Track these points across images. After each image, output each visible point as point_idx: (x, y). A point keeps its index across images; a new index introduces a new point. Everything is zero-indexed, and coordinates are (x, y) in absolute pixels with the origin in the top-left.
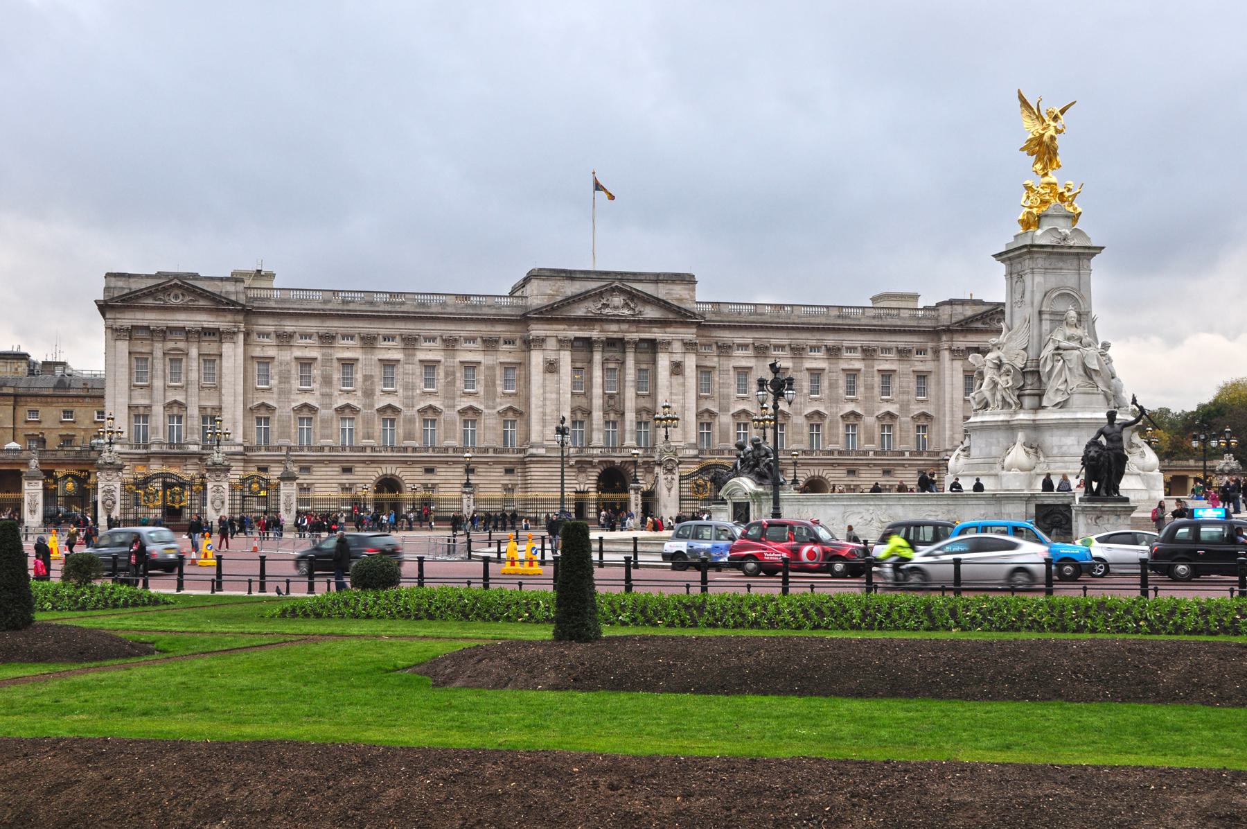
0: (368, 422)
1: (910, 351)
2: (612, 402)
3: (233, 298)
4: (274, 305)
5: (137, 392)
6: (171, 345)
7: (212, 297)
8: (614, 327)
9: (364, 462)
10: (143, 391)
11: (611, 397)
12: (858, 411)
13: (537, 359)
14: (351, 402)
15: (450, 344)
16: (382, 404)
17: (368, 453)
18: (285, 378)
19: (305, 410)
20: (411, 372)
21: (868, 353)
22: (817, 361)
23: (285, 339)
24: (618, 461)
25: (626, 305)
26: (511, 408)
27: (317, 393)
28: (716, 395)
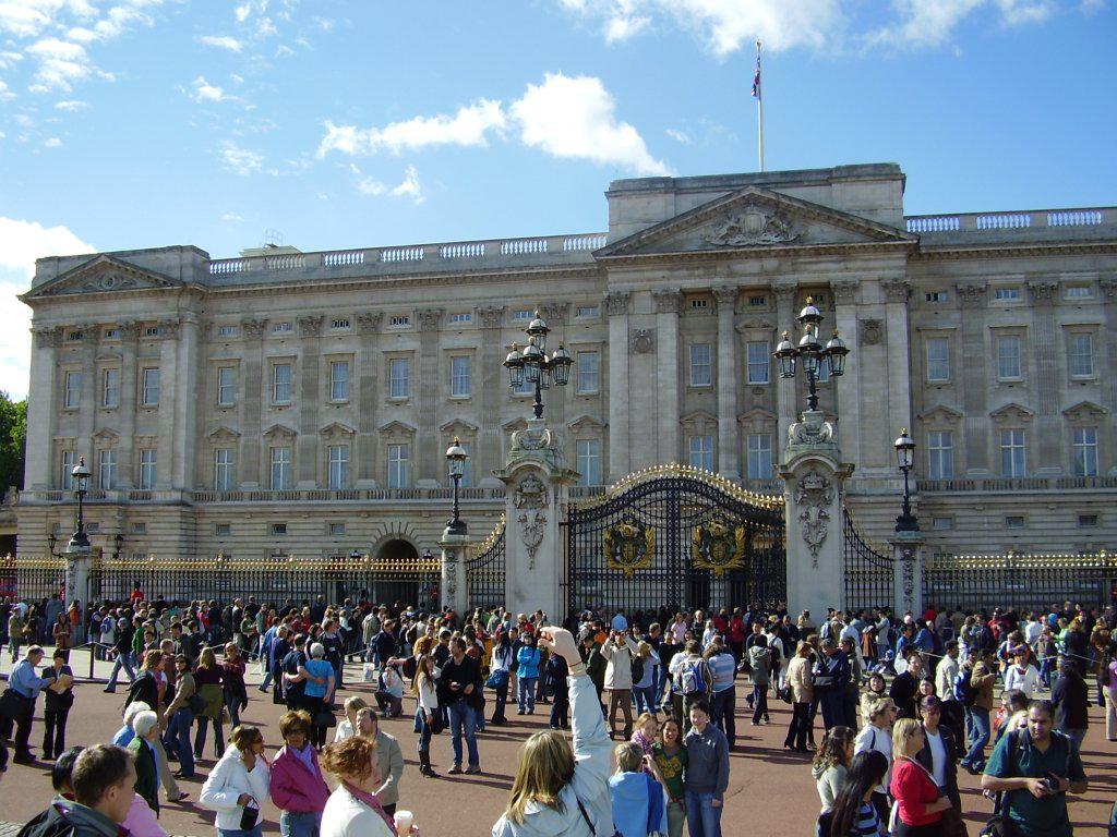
0: (368, 450)
2: (758, 400)
3: (175, 274)
5: (66, 420)
8: (753, 266)
9: (357, 514)
11: (758, 390)
14: (340, 421)
15: (492, 318)
16: (385, 422)
17: (363, 501)
18: (254, 389)
19: (280, 435)
23: (255, 329)
25: (771, 227)
26: (586, 419)
27: (297, 410)
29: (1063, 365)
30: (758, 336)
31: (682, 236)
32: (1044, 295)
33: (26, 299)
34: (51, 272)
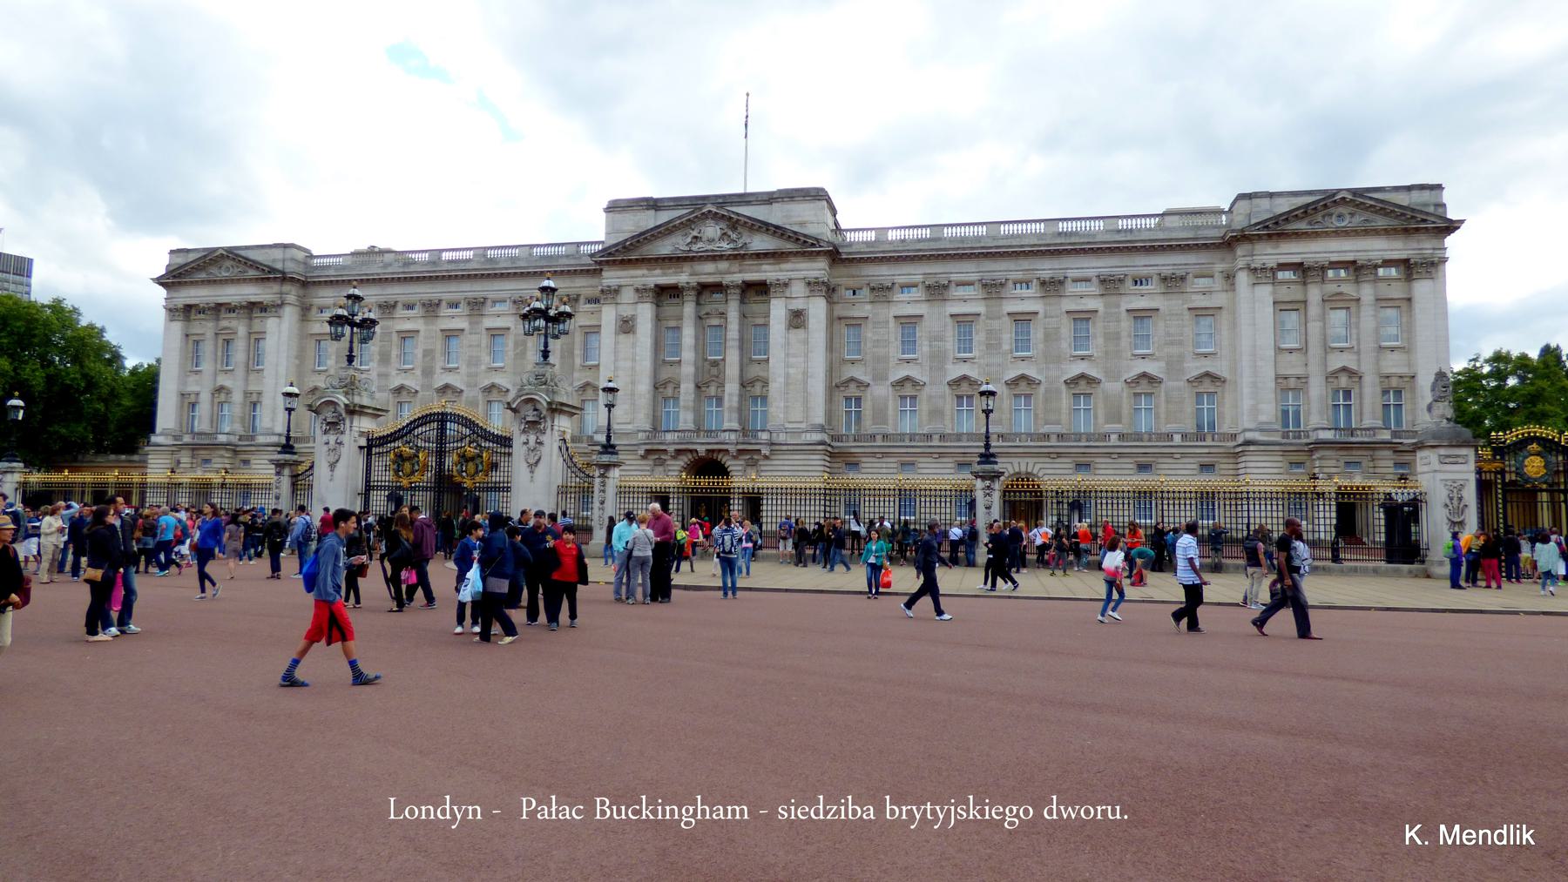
1: (1183, 278)
2: (714, 371)
3: (279, 266)
4: (332, 272)
5: (193, 378)
6: (224, 323)
7: (255, 265)
8: (709, 267)
10: (196, 377)
11: (715, 364)
12: (1093, 373)
13: (609, 315)
14: (407, 383)
16: (439, 383)
20: (473, 342)
21: (1110, 284)
22: (1026, 300)
24: (702, 450)
28: (868, 357)
29: (950, 344)
30: (715, 322)
31: (659, 243)
32: (937, 291)
33: (160, 281)
34: (180, 260)
